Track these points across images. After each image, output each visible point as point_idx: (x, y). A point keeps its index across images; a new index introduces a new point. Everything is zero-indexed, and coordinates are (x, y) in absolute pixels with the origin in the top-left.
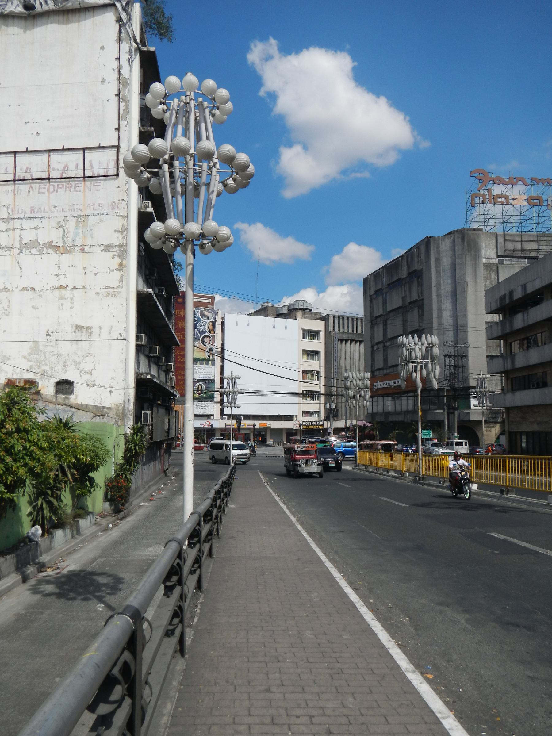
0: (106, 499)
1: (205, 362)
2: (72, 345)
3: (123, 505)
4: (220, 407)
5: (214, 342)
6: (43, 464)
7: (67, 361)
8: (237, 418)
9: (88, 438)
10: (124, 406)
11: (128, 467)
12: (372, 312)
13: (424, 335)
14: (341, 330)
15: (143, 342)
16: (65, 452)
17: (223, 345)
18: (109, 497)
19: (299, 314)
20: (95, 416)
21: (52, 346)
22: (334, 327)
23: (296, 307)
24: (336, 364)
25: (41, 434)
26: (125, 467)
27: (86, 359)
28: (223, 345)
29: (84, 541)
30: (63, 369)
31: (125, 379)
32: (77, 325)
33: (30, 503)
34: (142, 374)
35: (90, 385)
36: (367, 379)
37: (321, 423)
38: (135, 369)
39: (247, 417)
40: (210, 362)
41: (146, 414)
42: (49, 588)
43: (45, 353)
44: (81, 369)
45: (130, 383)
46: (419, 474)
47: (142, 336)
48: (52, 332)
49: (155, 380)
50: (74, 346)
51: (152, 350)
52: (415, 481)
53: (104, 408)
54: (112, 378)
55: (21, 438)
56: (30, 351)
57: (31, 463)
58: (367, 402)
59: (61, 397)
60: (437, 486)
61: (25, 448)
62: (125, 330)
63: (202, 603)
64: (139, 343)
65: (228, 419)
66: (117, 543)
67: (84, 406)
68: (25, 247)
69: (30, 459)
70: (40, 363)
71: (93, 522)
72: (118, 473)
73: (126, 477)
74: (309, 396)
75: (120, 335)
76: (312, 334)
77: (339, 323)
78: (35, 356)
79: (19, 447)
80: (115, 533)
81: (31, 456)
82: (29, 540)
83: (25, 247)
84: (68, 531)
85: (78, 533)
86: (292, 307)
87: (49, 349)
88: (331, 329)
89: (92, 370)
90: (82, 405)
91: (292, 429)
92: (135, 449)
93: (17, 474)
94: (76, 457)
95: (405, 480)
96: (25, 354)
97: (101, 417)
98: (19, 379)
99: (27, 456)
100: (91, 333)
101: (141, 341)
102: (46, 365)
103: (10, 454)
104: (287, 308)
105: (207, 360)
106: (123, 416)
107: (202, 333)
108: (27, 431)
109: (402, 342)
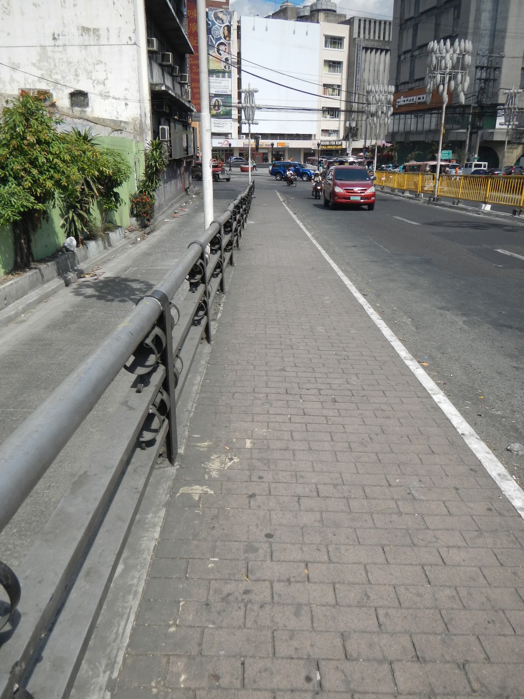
0: (132, 214)
1: (221, 75)
2: (81, 51)
3: (148, 220)
4: (238, 125)
5: (229, 49)
6: (68, 177)
7: (79, 70)
8: (255, 136)
9: (110, 153)
10: (141, 120)
11: (150, 184)
12: (402, 13)
13: (457, 40)
14: (367, 37)
15: (155, 48)
16: (88, 165)
17: (239, 54)
18: (135, 212)
19: (321, 16)
20: (113, 131)
21: (60, 52)
22: (359, 33)
23: (319, 7)
24: (358, 77)
25: (61, 146)
26: (147, 184)
27: (98, 67)
28: (239, 54)
29: (116, 252)
30: (75, 79)
31: (140, 90)
32: (83, 27)
33: (62, 216)
34: (156, 85)
35: (105, 96)
36: (390, 93)
37: (340, 143)
38: (149, 79)
39: (265, 136)
40: (226, 74)
41: (163, 129)
42: (90, 291)
43: (54, 60)
44: (93, 78)
45: (144, 94)
46: (434, 195)
47: (153, 41)
48: (59, 35)
49: (170, 92)
50: (83, 52)
51: (165, 57)
52: (429, 202)
53: (121, 122)
54: (126, 89)
55: (43, 150)
56: (38, 58)
57: (57, 176)
58: (388, 119)
59: (77, 109)
60: (450, 207)
61: (48, 160)
62: (134, 32)
63: (224, 303)
64: (151, 49)
65: (246, 138)
66: (146, 254)
67: (101, 120)
69: (55, 172)
70: (51, 72)
71: (123, 235)
72: (141, 189)
73: (149, 193)
74: (328, 114)
75: (130, 38)
77: (364, 28)
78: (45, 63)
79: (42, 160)
80: (143, 246)
81: (55, 168)
82: (66, 249)
84: (100, 242)
85: (110, 245)
86: (315, 8)
87: (58, 56)
88: (355, 35)
89: (105, 79)
90: (99, 119)
91: (310, 149)
92: (156, 165)
93: (45, 186)
94: (99, 171)
95: (420, 201)
96: (34, 61)
97: (119, 132)
98: (33, 90)
99: (52, 168)
100: (99, 36)
101: (153, 46)
102: (57, 73)
103: (35, 167)
104: (308, 8)
105: (224, 72)
106: (141, 131)
107: (217, 40)
108: (48, 143)
109: (433, 48)
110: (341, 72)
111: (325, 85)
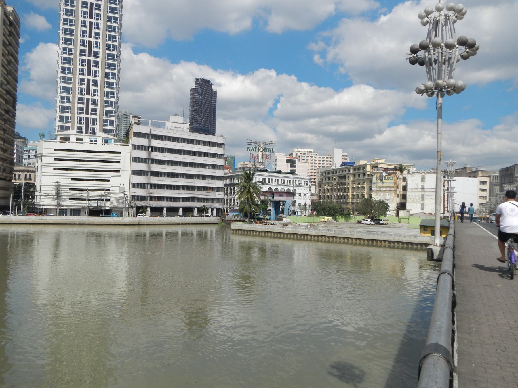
22: (493, 180)
68: (430, 199)
76: (484, 183)
77: (495, 179)
83: (430, 199)
86: (477, 169)
88: (492, 181)
110: (486, 192)
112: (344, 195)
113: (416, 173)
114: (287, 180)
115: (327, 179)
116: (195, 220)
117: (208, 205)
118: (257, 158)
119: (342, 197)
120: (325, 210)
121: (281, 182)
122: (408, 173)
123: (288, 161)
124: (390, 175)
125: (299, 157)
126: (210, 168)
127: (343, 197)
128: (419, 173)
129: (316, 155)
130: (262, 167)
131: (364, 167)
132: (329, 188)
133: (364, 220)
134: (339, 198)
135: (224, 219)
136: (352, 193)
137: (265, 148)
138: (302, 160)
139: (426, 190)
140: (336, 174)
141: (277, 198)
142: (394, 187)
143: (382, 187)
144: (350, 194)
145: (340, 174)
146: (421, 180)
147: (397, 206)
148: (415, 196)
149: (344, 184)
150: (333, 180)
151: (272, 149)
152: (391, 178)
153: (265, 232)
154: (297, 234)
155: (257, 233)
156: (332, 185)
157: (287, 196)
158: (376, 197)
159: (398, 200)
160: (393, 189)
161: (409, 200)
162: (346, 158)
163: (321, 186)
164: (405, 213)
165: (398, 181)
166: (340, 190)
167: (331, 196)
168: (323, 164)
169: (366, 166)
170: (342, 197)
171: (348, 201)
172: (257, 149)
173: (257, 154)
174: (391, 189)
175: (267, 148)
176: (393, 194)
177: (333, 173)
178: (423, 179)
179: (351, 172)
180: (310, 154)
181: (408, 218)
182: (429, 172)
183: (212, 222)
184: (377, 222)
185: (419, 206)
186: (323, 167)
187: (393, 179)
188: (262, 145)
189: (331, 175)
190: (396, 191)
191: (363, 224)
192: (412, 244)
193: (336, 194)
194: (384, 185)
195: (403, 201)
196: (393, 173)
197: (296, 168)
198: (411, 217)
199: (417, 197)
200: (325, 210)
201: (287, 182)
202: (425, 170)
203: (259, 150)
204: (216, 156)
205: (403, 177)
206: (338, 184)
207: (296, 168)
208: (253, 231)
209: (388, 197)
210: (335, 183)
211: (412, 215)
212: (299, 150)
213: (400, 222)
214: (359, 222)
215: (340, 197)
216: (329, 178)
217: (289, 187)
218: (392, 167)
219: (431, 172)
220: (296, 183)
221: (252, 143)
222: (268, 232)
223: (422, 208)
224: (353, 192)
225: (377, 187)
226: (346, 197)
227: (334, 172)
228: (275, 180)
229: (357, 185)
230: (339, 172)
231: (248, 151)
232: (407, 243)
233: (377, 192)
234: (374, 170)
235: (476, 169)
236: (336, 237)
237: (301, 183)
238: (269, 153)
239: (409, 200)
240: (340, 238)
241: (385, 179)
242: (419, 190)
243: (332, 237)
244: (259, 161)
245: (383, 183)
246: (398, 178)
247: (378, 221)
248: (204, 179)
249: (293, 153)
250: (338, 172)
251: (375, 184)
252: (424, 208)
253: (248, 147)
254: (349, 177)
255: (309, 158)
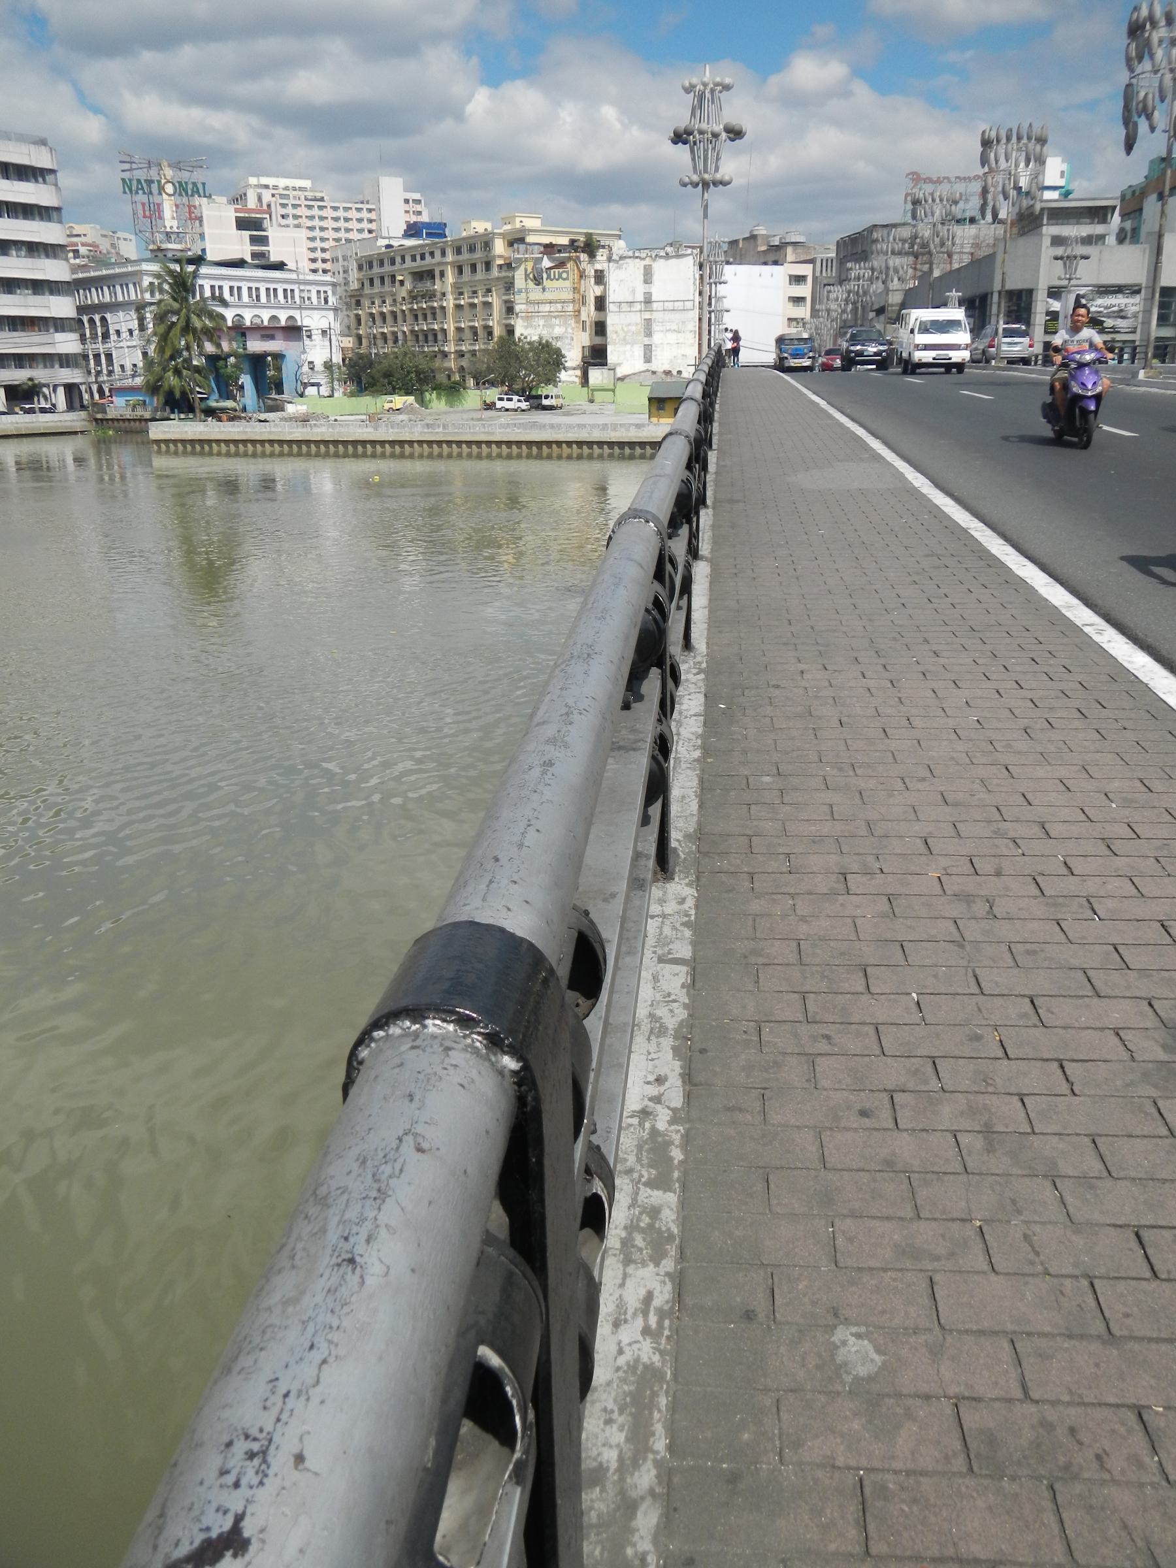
12: (840, 276)
68: (667, 331)
76: (798, 279)
83: (667, 331)
86: (783, 241)
88: (818, 274)
104: (777, 238)
110: (805, 306)
111: (789, 319)
112: (434, 330)
113: (630, 257)
114: (268, 289)
115: (377, 282)
116: (12, 423)
117: (40, 374)
118: (161, 218)
119: (426, 336)
120: (393, 376)
121: (250, 296)
122: (610, 259)
123: (242, 224)
124: (561, 264)
125: (269, 206)
126: (23, 253)
127: (430, 338)
128: (637, 257)
129: (322, 199)
130: (178, 247)
131: (487, 243)
132: (385, 310)
133: (501, 399)
134: (417, 341)
135: (99, 416)
136: (456, 325)
137: (180, 183)
138: (280, 218)
139: (655, 306)
140: (405, 266)
141: (255, 346)
142: (573, 301)
143: (542, 303)
144: (450, 327)
145: (414, 264)
146: (642, 278)
147: (583, 357)
148: (629, 325)
149: (431, 296)
150: (397, 284)
151: (204, 184)
152: (564, 275)
153: (254, 442)
154: (345, 443)
155: (231, 445)
156: (394, 300)
157: (287, 339)
158: (527, 331)
159: (585, 339)
160: (570, 307)
161: (614, 337)
162: (418, 208)
163: (358, 303)
164: (605, 375)
165: (582, 281)
166: (420, 317)
167: (394, 334)
168: (348, 230)
169: (492, 240)
170: (426, 336)
171: (446, 349)
172: (155, 187)
173: (159, 205)
174: (566, 309)
175: (186, 183)
176: (572, 322)
177: (393, 262)
178: (648, 277)
179: (450, 257)
180: (302, 194)
181: (612, 387)
182: (662, 253)
183: (66, 427)
184: (536, 403)
185: (639, 351)
186: (348, 241)
187: (571, 278)
188: (169, 173)
189: (387, 268)
190: (579, 311)
191: (500, 410)
192: (632, 445)
193: (410, 328)
194: (548, 296)
195: (598, 340)
196: (570, 258)
197: (267, 245)
198: (619, 384)
199: (633, 328)
200: (393, 376)
201: (268, 295)
202: (652, 249)
203: (161, 189)
204: (36, 212)
205: (596, 271)
206: (413, 297)
207: (267, 245)
208: (218, 441)
209: (558, 331)
210: (403, 292)
211: (621, 379)
212: (264, 180)
213: (592, 401)
214: (490, 406)
215: (421, 338)
216: (382, 279)
217: (274, 312)
218: (564, 241)
219: (667, 254)
220: (293, 297)
221: (134, 166)
222: (262, 442)
223: (648, 359)
224: (460, 322)
225: (529, 302)
226: (440, 337)
227: (398, 259)
228: (231, 288)
229: (469, 298)
230: (414, 259)
231: (125, 192)
232: (621, 445)
233: (528, 317)
234: (518, 252)
235: (781, 239)
236: (449, 443)
237: (309, 298)
238: (197, 201)
239: (614, 337)
240: (459, 443)
241: (549, 277)
242: (638, 307)
243: (439, 443)
244: (165, 227)
245: (544, 289)
246: (582, 275)
247: (536, 402)
248: (10, 292)
249: (245, 194)
250: (408, 259)
251: (523, 295)
252: (651, 357)
253: (123, 180)
254: (442, 274)
255: (302, 211)
